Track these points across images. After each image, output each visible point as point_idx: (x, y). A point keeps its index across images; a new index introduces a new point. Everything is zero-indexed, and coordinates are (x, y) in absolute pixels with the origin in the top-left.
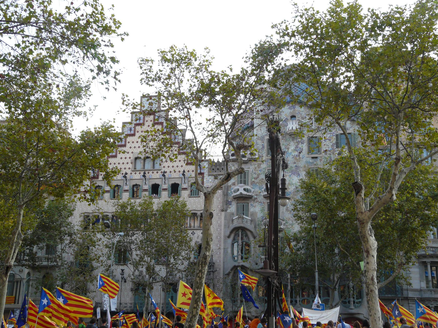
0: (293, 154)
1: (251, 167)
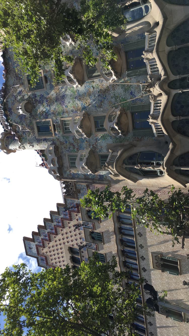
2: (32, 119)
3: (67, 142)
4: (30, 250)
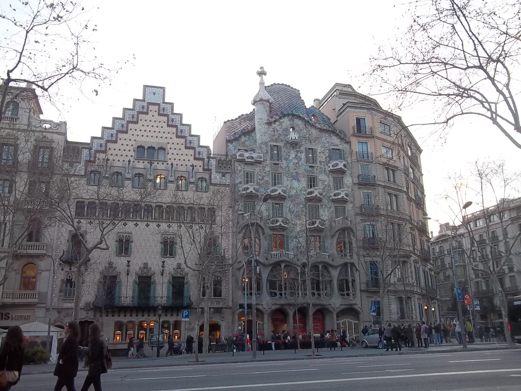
0: (294, 161)
1: (256, 169)
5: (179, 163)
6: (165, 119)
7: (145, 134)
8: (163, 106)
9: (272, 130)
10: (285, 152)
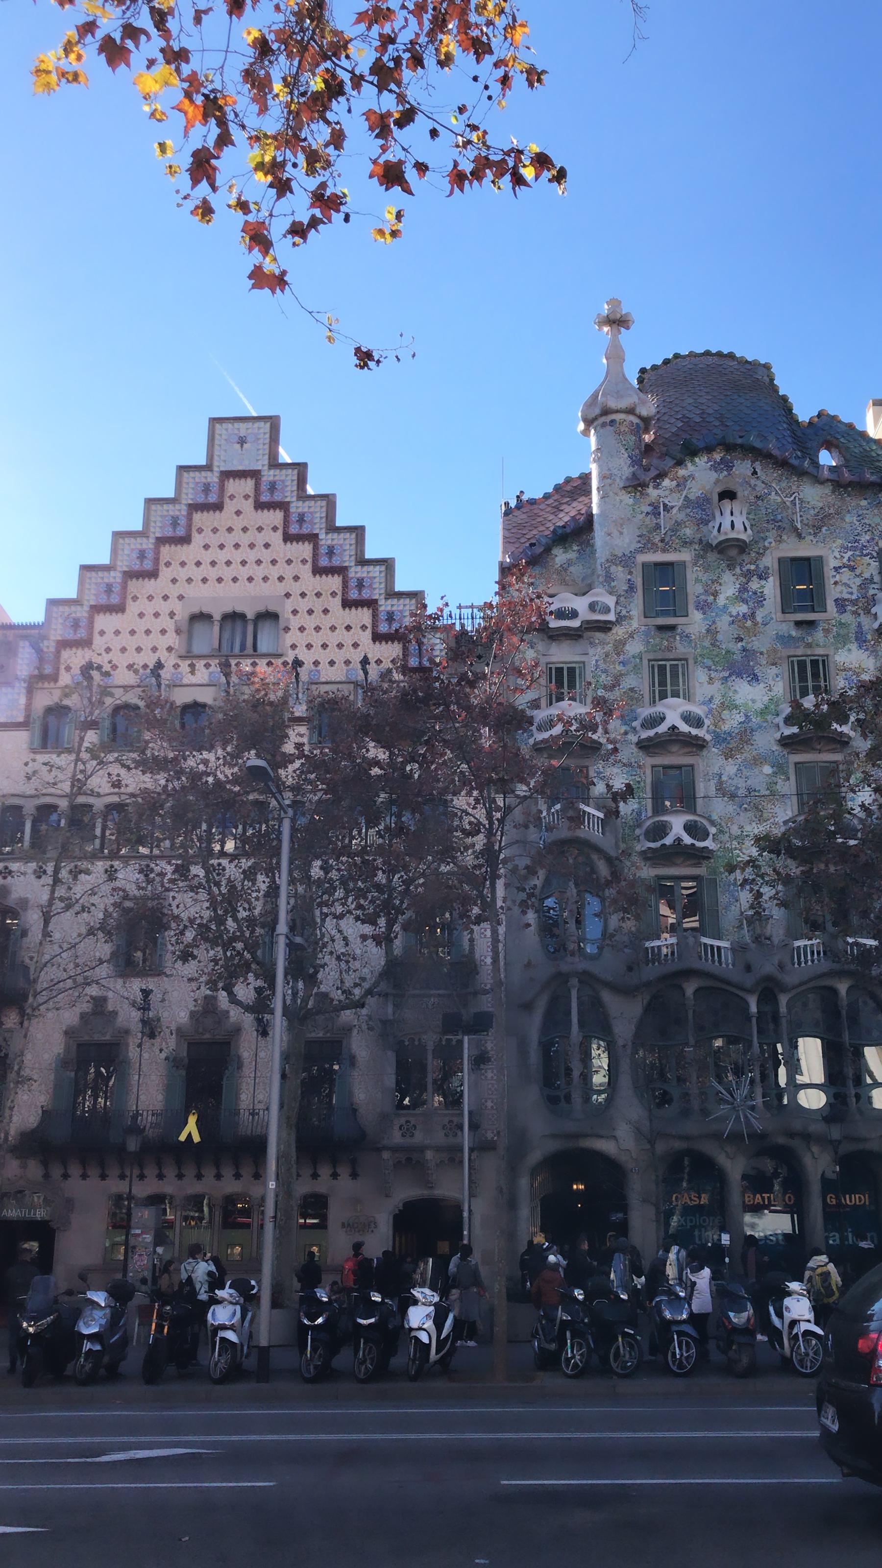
2: (695, 550)
3: (624, 666)
4: (236, 439)
5: (324, 657)
6: (276, 517)
7: (212, 574)
8: (269, 475)
9: (649, 509)
10: (697, 580)
